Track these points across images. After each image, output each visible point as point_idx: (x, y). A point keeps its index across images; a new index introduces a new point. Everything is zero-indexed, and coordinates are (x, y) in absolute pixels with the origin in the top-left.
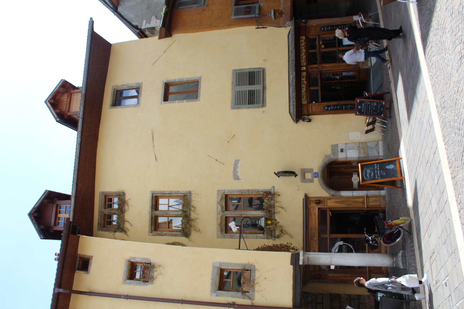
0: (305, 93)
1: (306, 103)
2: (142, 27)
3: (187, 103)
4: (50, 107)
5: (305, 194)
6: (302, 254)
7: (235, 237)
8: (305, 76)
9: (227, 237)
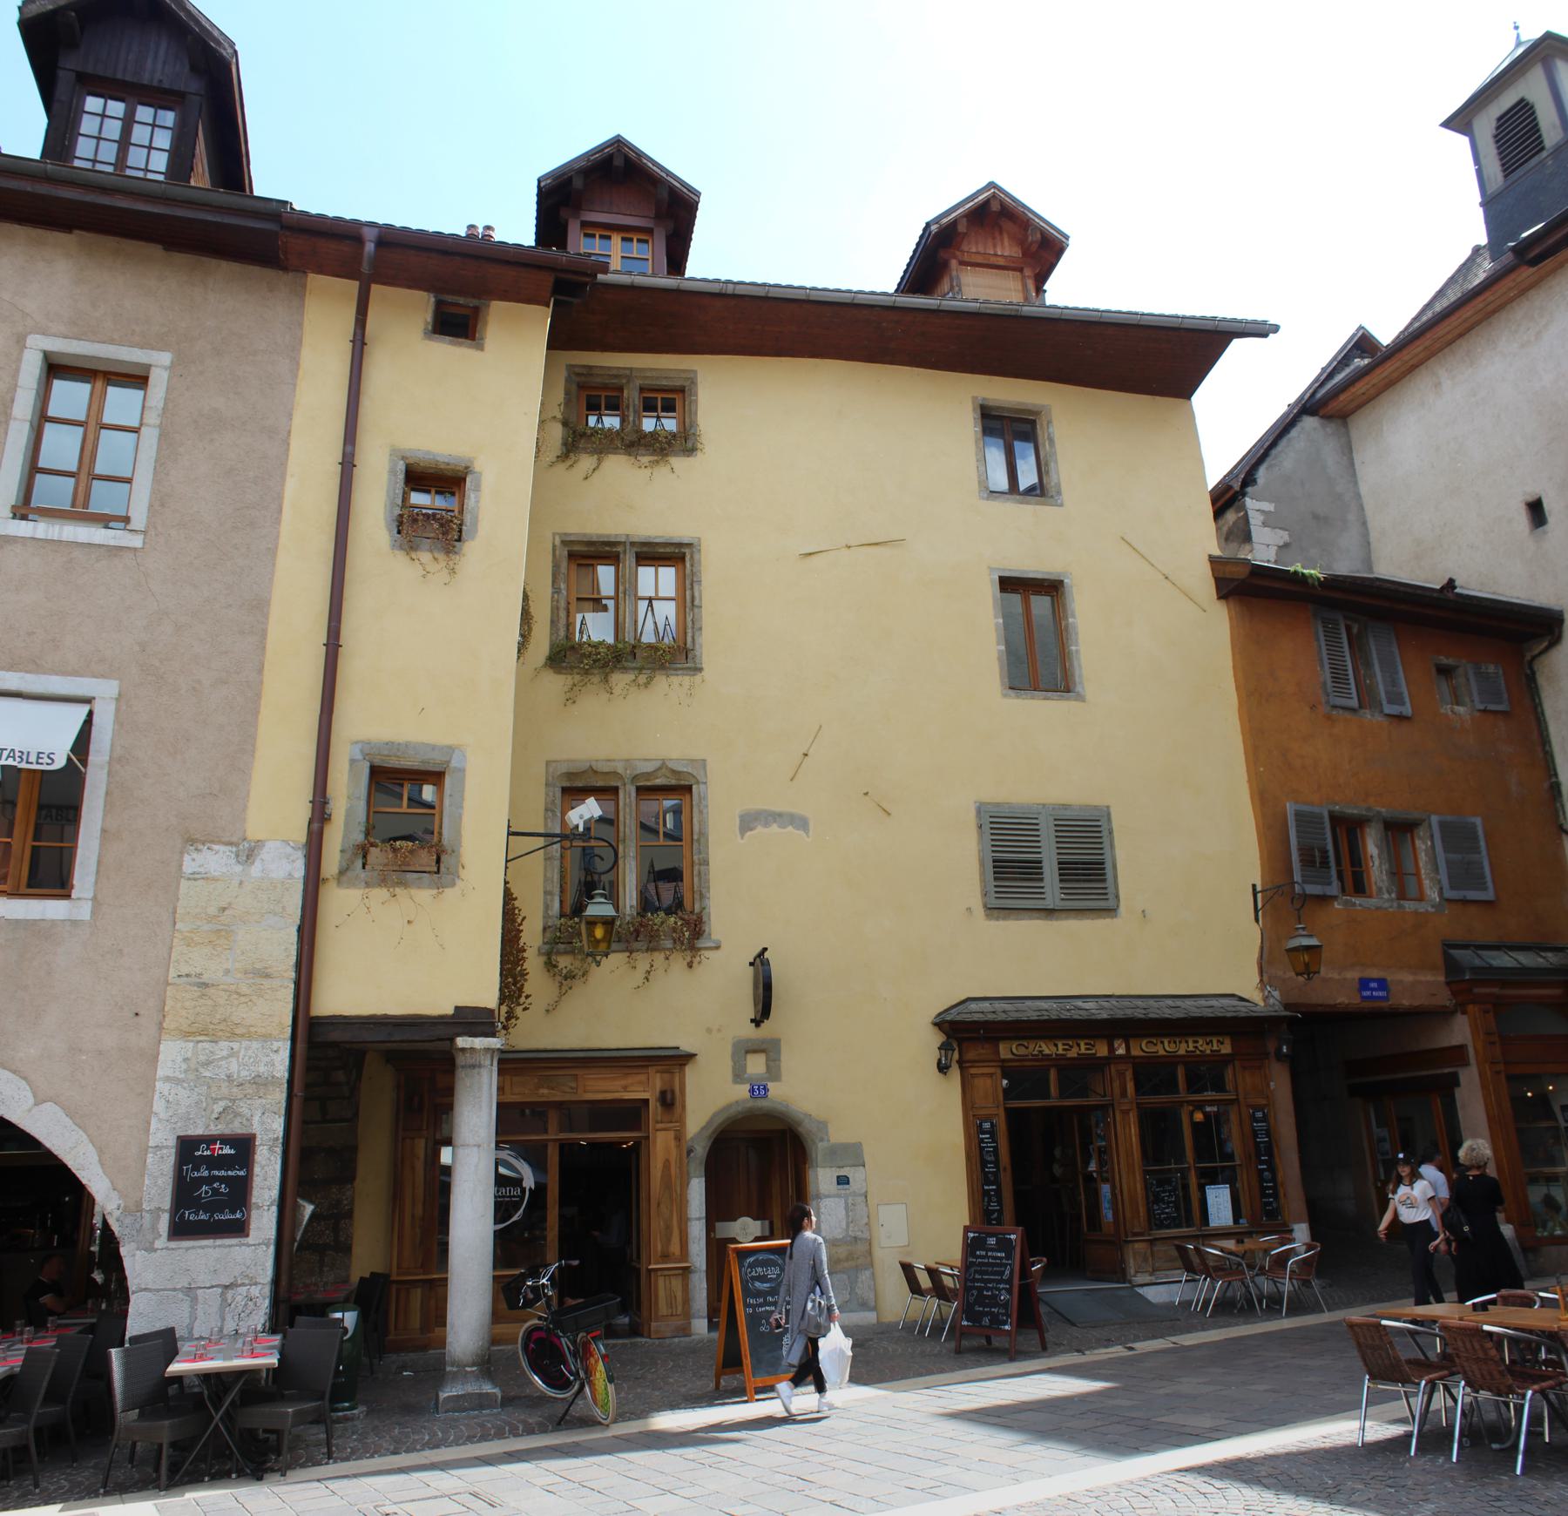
0: (1036, 1052)
1: (1002, 1057)
3: (995, 655)
5: (693, 1051)
9: (551, 794)
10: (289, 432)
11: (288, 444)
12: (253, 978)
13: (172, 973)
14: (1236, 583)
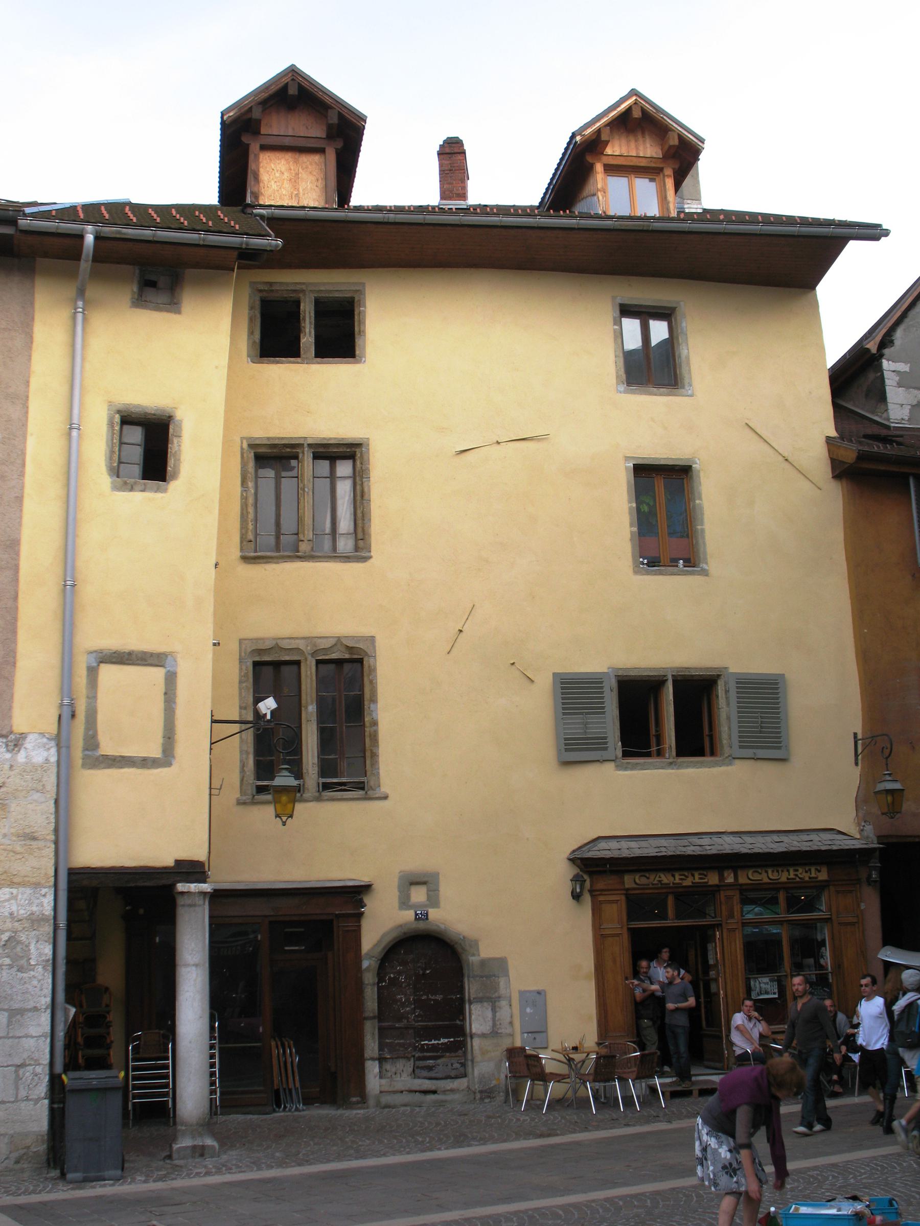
0: (656, 882)
1: (627, 886)
2: (888, 360)
3: (628, 536)
4: (619, 109)
6: (205, 891)
7: (243, 691)
8: (706, 880)
10: (27, 397)
11: (28, 407)
12: (24, 840)
14: (846, 466)
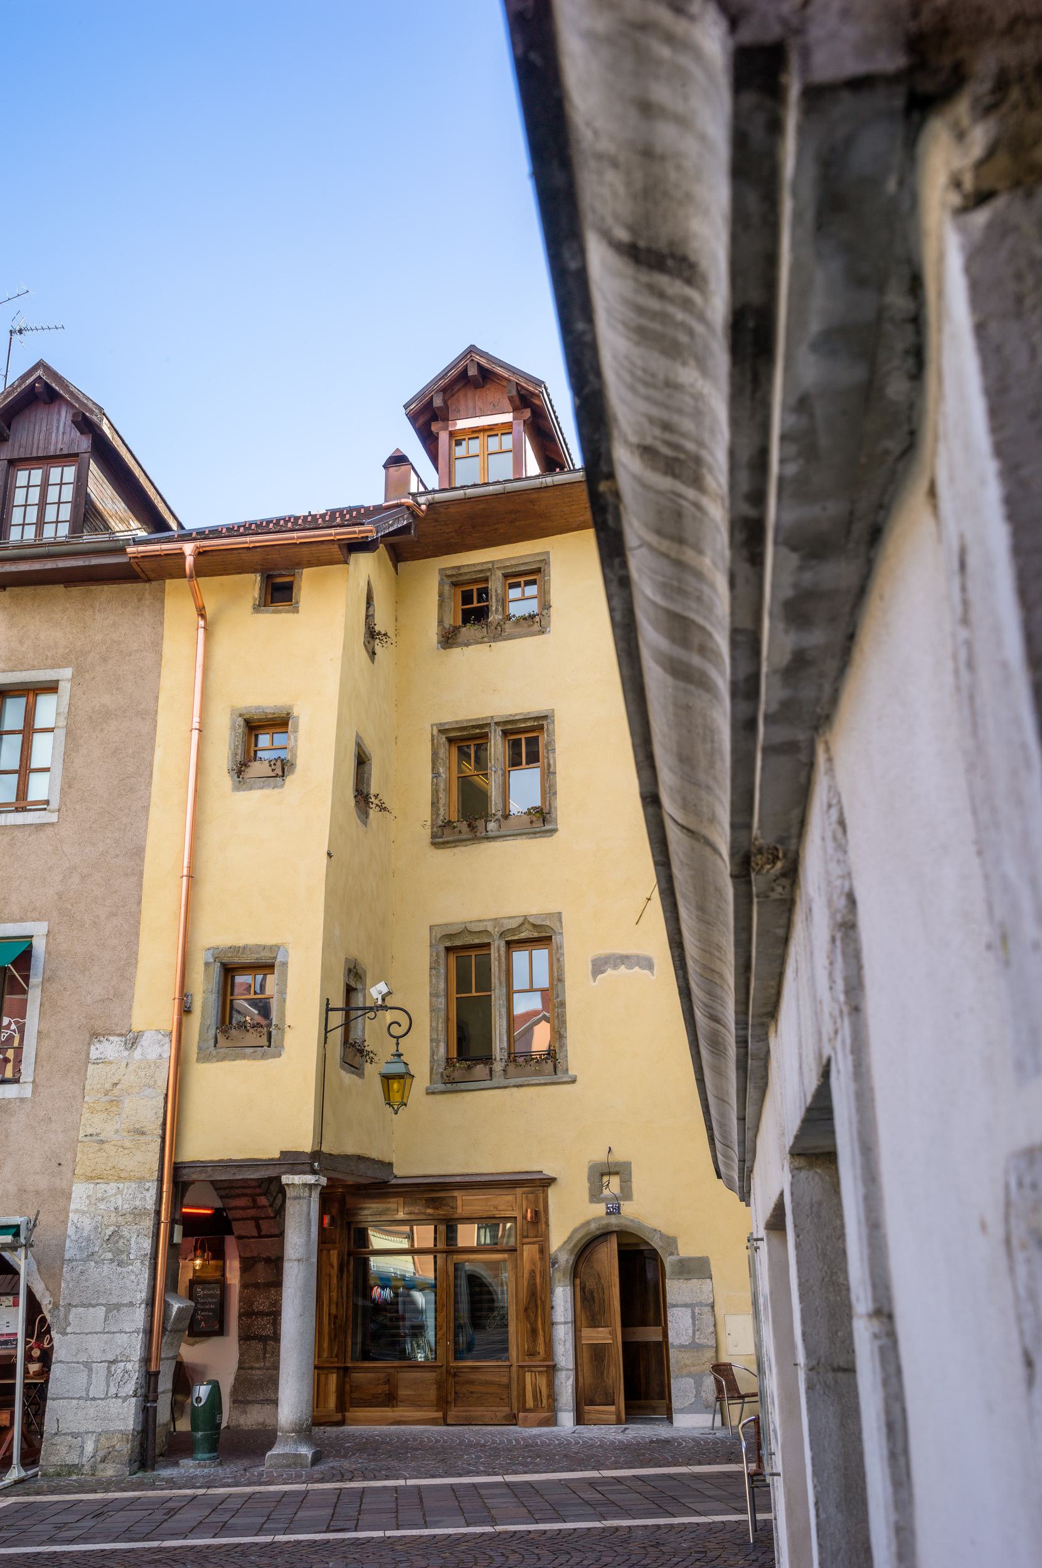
5: (553, 1175)
9: (434, 954)
11: (156, 721)
13: (82, 1134)
